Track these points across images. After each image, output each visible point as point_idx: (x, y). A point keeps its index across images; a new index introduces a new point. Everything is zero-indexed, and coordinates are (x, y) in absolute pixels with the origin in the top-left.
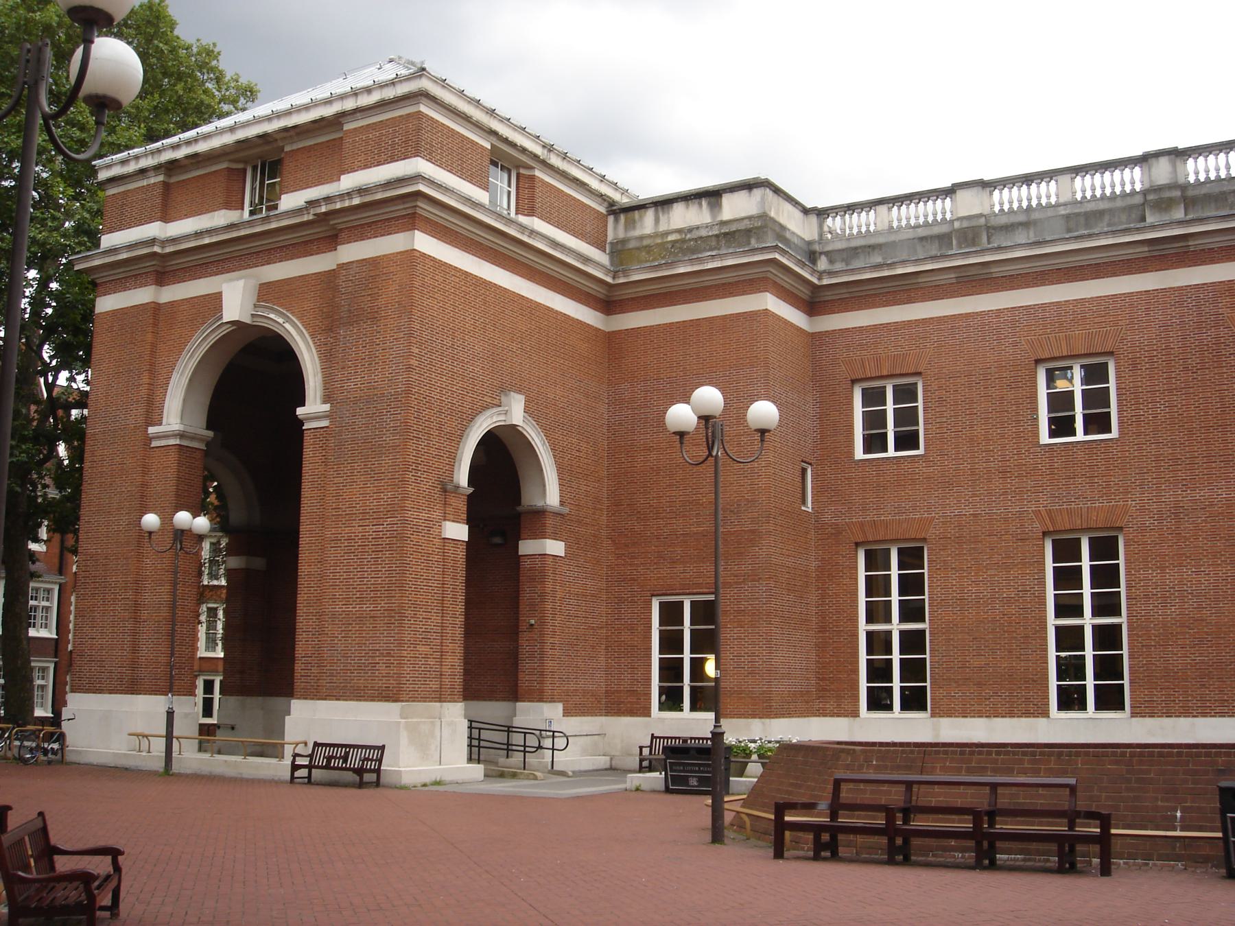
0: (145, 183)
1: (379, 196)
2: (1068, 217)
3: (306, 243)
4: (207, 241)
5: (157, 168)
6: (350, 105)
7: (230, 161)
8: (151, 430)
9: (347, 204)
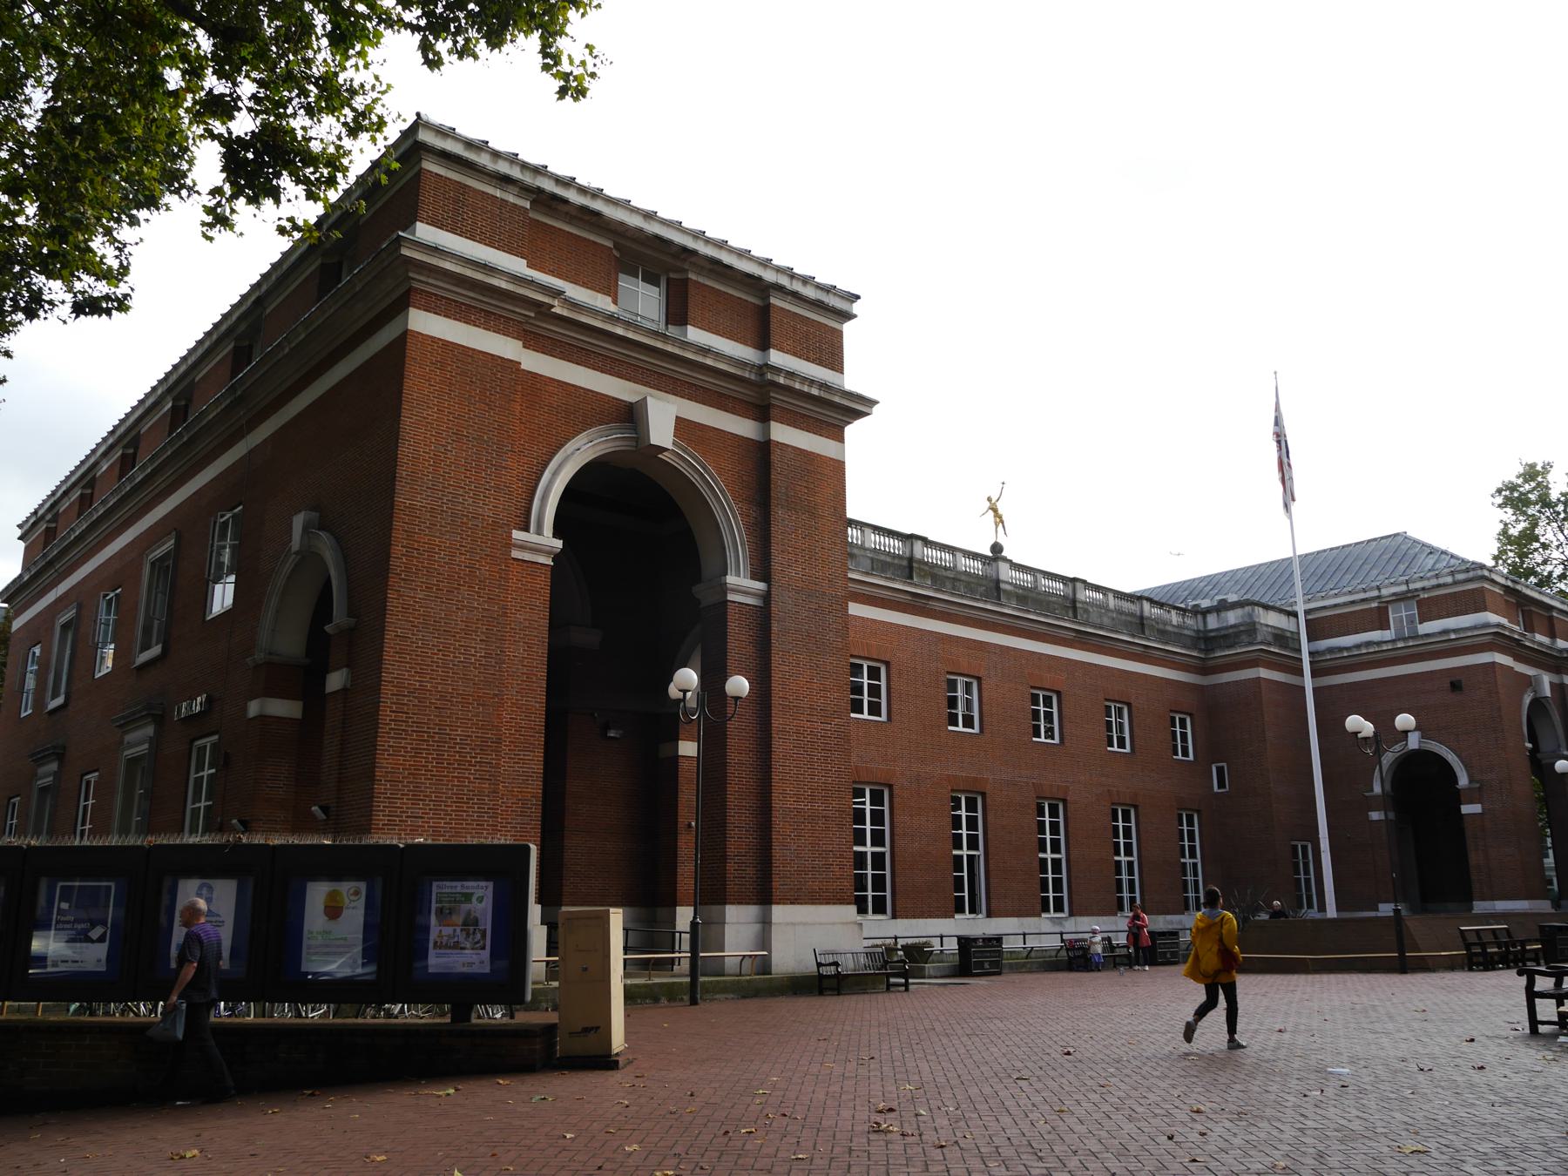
0: (498, 193)
1: (837, 399)
2: (872, 560)
3: (721, 395)
4: (620, 331)
5: (526, 190)
6: (784, 281)
7: (617, 246)
8: (517, 535)
9: (806, 389)
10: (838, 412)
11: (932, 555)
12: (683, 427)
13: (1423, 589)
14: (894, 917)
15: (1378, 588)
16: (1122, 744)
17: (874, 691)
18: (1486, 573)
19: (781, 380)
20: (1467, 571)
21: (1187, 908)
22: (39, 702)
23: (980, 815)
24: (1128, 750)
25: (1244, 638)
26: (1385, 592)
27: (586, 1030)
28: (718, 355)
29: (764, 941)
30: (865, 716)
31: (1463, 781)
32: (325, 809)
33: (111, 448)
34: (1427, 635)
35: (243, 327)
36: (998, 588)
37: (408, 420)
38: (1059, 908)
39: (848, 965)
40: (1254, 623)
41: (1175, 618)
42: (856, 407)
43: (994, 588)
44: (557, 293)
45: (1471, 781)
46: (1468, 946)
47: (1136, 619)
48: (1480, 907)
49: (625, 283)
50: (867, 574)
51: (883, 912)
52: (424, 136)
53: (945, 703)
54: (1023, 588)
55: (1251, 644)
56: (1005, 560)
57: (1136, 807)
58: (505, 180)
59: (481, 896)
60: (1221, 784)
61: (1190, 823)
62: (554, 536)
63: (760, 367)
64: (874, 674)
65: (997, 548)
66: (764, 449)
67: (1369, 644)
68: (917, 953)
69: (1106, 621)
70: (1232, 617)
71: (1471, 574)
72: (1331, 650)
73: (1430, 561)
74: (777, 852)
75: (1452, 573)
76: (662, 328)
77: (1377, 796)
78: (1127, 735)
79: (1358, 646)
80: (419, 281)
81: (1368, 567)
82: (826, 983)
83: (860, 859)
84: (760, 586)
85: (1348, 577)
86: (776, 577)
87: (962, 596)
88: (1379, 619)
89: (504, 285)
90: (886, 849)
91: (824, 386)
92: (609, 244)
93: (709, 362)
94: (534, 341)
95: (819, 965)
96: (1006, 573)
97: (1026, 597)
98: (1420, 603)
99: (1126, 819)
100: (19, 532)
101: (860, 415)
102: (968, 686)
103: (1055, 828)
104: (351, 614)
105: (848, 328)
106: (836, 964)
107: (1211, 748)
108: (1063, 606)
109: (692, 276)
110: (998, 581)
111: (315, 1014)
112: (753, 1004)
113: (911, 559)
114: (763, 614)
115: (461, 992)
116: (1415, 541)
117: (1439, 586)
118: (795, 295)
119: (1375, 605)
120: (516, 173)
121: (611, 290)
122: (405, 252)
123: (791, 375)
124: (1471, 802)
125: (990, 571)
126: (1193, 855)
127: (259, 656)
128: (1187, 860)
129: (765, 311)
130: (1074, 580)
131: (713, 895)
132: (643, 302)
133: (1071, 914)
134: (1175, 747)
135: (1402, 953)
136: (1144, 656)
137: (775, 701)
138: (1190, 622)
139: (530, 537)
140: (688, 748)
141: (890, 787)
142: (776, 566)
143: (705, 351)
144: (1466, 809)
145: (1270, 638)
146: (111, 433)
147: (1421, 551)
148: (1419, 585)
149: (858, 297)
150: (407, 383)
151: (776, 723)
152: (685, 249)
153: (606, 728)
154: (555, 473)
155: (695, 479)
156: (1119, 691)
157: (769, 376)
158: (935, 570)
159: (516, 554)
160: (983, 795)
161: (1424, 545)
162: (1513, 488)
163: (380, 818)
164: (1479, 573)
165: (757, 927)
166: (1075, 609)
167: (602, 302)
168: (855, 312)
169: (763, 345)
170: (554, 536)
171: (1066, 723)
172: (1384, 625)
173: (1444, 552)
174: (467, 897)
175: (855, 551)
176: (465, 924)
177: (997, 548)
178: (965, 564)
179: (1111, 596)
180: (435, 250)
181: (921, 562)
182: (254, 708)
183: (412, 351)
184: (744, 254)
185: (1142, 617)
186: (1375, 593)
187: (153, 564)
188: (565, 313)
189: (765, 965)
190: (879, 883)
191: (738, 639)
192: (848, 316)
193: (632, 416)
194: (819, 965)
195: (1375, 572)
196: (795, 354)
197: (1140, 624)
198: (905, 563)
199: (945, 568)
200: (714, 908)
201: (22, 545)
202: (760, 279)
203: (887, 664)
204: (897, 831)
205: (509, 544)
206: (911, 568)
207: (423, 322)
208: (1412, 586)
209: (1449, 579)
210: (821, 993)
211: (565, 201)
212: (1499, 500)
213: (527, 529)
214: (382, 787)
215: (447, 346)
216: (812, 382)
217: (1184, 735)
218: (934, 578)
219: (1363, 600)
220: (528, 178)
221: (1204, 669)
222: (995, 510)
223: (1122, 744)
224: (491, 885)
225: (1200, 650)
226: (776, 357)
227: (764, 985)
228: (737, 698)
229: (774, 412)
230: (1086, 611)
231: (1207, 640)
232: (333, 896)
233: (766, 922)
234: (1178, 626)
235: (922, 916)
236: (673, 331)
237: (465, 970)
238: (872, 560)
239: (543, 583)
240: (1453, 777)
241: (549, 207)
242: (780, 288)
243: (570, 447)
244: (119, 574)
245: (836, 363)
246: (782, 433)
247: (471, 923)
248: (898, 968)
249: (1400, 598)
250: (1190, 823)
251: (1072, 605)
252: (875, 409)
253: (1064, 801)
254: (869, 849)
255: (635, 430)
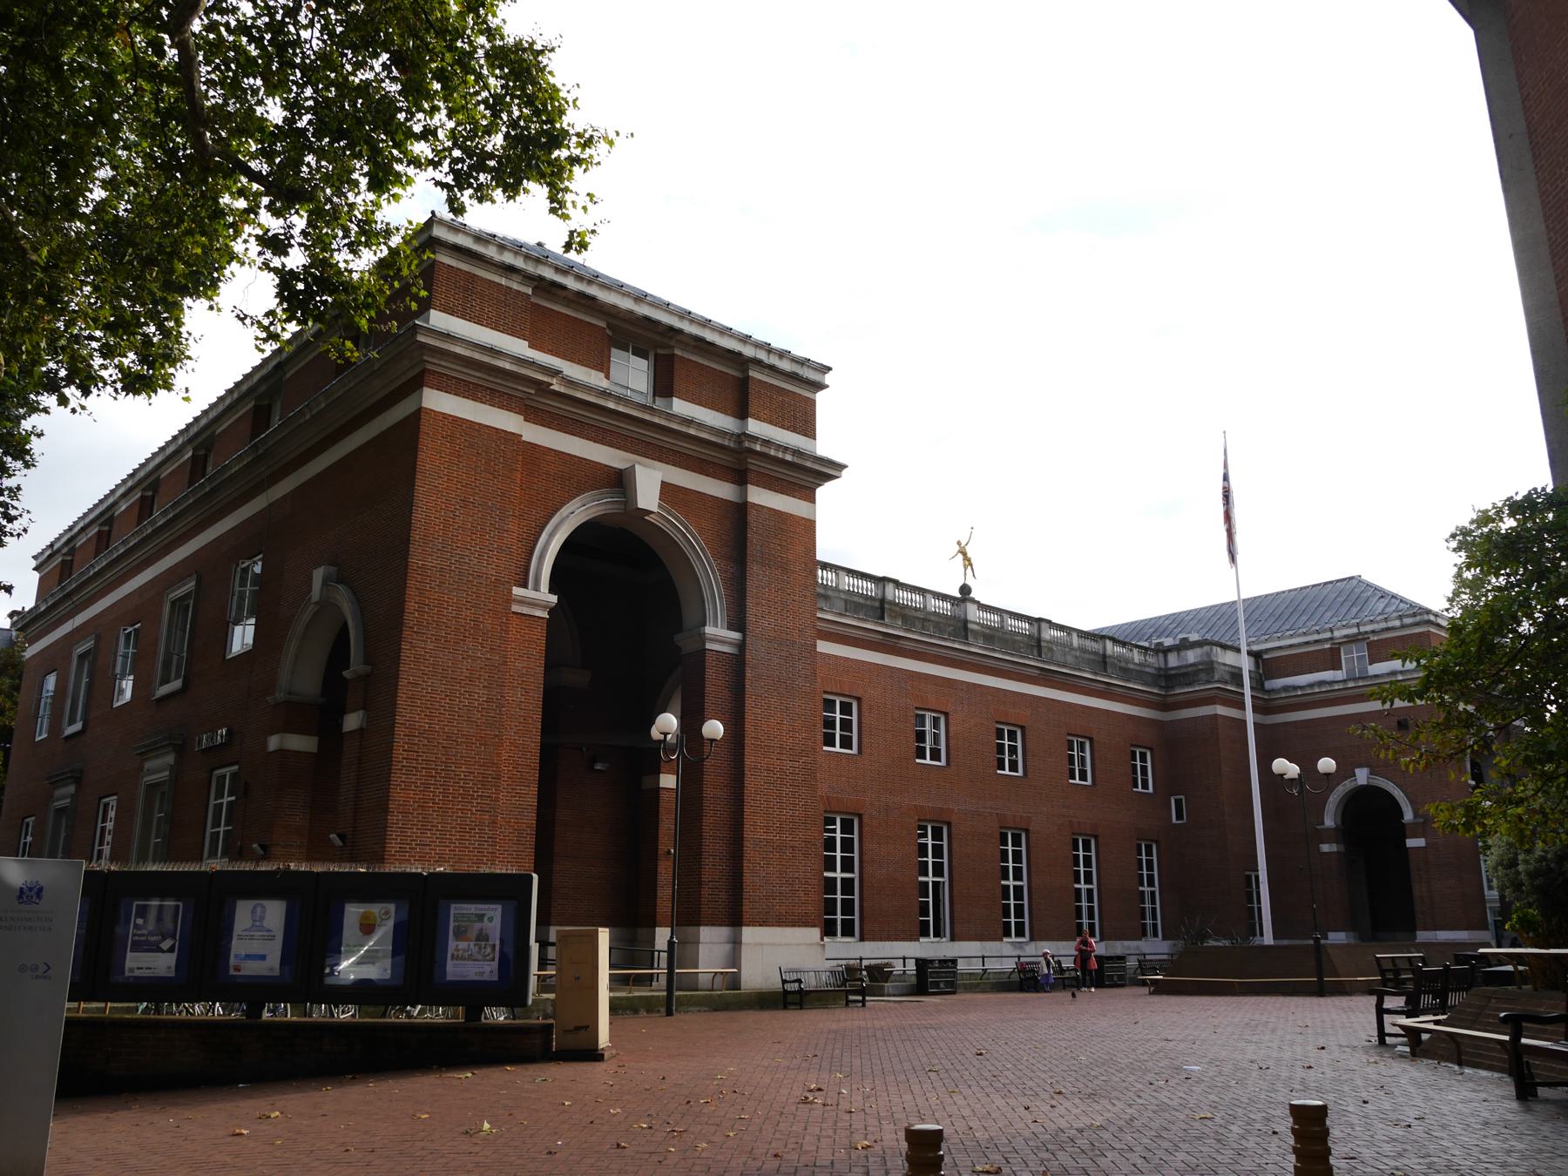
0: (503, 281)
1: (808, 464)
2: (846, 601)
4: (611, 405)
5: (528, 278)
6: (762, 355)
7: (609, 325)
8: (517, 591)
9: (780, 455)
10: (810, 474)
11: (903, 597)
12: (669, 492)
13: (1373, 632)
14: (862, 939)
15: (1331, 630)
16: (1083, 777)
17: (846, 725)
18: (1432, 618)
19: (758, 448)
20: (1414, 615)
21: (1144, 934)
22: (55, 728)
23: (945, 843)
24: (1089, 782)
25: (1203, 676)
26: (1337, 634)
27: (578, 1029)
28: (701, 426)
29: (735, 959)
30: (837, 749)
31: (1408, 816)
32: (342, 837)
33: (131, 489)
34: (1376, 676)
35: (263, 388)
36: (966, 628)
37: (421, 489)
38: (1020, 933)
39: (810, 983)
40: (1212, 662)
41: (1137, 656)
42: (827, 470)
43: (961, 628)
44: (555, 373)
45: (1416, 815)
46: (1383, 972)
47: (1098, 656)
48: (1423, 936)
49: (618, 357)
50: (840, 615)
51: (852, 935)
52: (438, 232)
53: (913, 736)
54: (990, 628)
55: (1209, 682)
56: (973, 601)
57: (1096, 837)
58: (510, 270)
59: (492, 917)
60: (1179, 816)
61: (1149, 853)
62: (551, 591)
63: (739, 436)
64: (846, 709)
65: (965, 590)
66: (741, 509)
67: (1321, 683)
68: (879, 973)
69: (1070, 659)
70: (1191, 656)
71: (1418, 619)
72: (1286, 688)
73: (1381, 605)
74: (748, 877)
75: (1400, 617)
76: (649, 401)
77: (1328, 829)
78: (1089, 769)
79: (1311, 685)
80: (433, 364)
81: (1322, 609)
82: (791, 998)
83: (830, 885)
84: (735, 635)
85: (1304, 618)
86: (750, 627)
87: (931, 636)
88: (1331, 659)
89: (508, 366)
90: (855, 875)
91: (797, 452)
92: (602, 324)
93: (692, 432)
94: (534, 414)
95: (784, 982)
96: (973, 614)
97: (992, 636)
98: (1370, 645)
99: (1087, 848)
100: (34, 563)
101: (830, 477)
102: (936, 722)
103: (1017, 857)
104: (368, 660)
105: (821, 398)
106: (799, 981)
107: (1170, 782)
108: (1028, 645)
109: (677, 352)
110: (966, 622)
111: (346, 1014)
112: (722, 1016)
113: (883, 601)
114: (738, 661)
115: (473, 996)
116: (1369, 585)
117: (1388, 629)
118: (772, 368)
119: (1327, 646)
120: (519, 263)
121: (603, 366)
122: (421, 338)
123: (767, 443)
124: (1415, 836)
125: (959, 612)
126: (1151, 883)
127: (280, 696)
128: (1146, 889)
129: (744, 384)
130: (1040, 620)
131: (689, 917)
132: (632, 375)
133: (1032, 939)
134: (1135, 780)
135: (1320, 978)
136: (1106, 692)
137: (748, 741)
138: (1151, 660)
139: (528, 593)
140: (668, 781)
141: (860, 816)
142: (750, 618)
143: (689, 422)
144: (1411, 843)
145: (1227, 677)
146: (131, 476)
147: (1373, 595)
148: (1369, 628)
149: (830, 369)
150: (421, 456)
151: (749, 761)
152: (671, 329)
153: (594, 761)
154: (552, 535)
155: (678, 538)
156: (1080, 726)
157: (747, 444)
158: (907, 611)
159: (515, 608)
160: (949, 824)
161: (1376, 589)
162: (1465, 532)
163: (393, 846)
164: (1426, 617)
165: (728, 947)
166: (1039, 647)
167: (595, 378)
168: (827, 382)
169: (742, 414)
170: (551, 591)
171: (1029, 756)
172: (1336, 666)
173: (1394, 597)
174: (481, 917)
175: (830, 593)
176: (478, 939)
177: (965, 590)
178: (934, 605)
179: (1075, 635)
180: (448, 336)
181: (893, 603)
182: (274, 742)
183: (425, 427)
184: (726, 331)
185: (1104, 656)
186: (1328, 635)
187: (173, 603)
188: (562, 390)
189: (734, 982)
190: (848, 907)
191: (715, 684)
192: (821, 386)
193: (620, 482)
194: (784, 982)
195: (1329, 614)
196: (771, 423)
197: (1103, 662)
198: (877, 604)
199: (916, 609)
200: (690, 929)
201: (37, 575)
202: (740, 354)
203: (859, 699)
204: (866, 858)
205: (509, 599)
206: (882, 609)
207: (437, 401)
208: (1362, 629)
209: (1397, 623)
210: (785, 1008)
211: (564, 288)
212: (1454, 544)
213: (525, 586)
214: (394, 818)
215: (456, 421)
216: (786, 449)
217: (1144, 769)
218: (905, 618)
219: (1316, 641)
220: (530, 268)
221: (1164, 706)
222: (965, 554)
223: (1083, 777)
224: (499, 907)
225: (1161, 687)
226: (755, 427)
227: (733, 999)
228: (713, 740)
229: (751, 476)
230: (1051, 650)
231: (1168, 678)
232: (365, 916)
233: (736, 942)
234: (1140, 665)
235: (889, 939)
236: (660, 404)
237: (478, 978)
238: (846, 601)
239: (539, 635)
240: (1400, 814)
241: (549, 292)
242: (758, 363)
243: (565, 511)
244: (140, 609)
245: (808, 429)
246: (758, 496)
247: (482, 937)
248: (858, 985)
249: (1352, 640)
250: (1149, 853)
251: (1036, 644)
252: (844, 472)
253: (1027, 831)
254: (839, 875)
255: (624, 494)
